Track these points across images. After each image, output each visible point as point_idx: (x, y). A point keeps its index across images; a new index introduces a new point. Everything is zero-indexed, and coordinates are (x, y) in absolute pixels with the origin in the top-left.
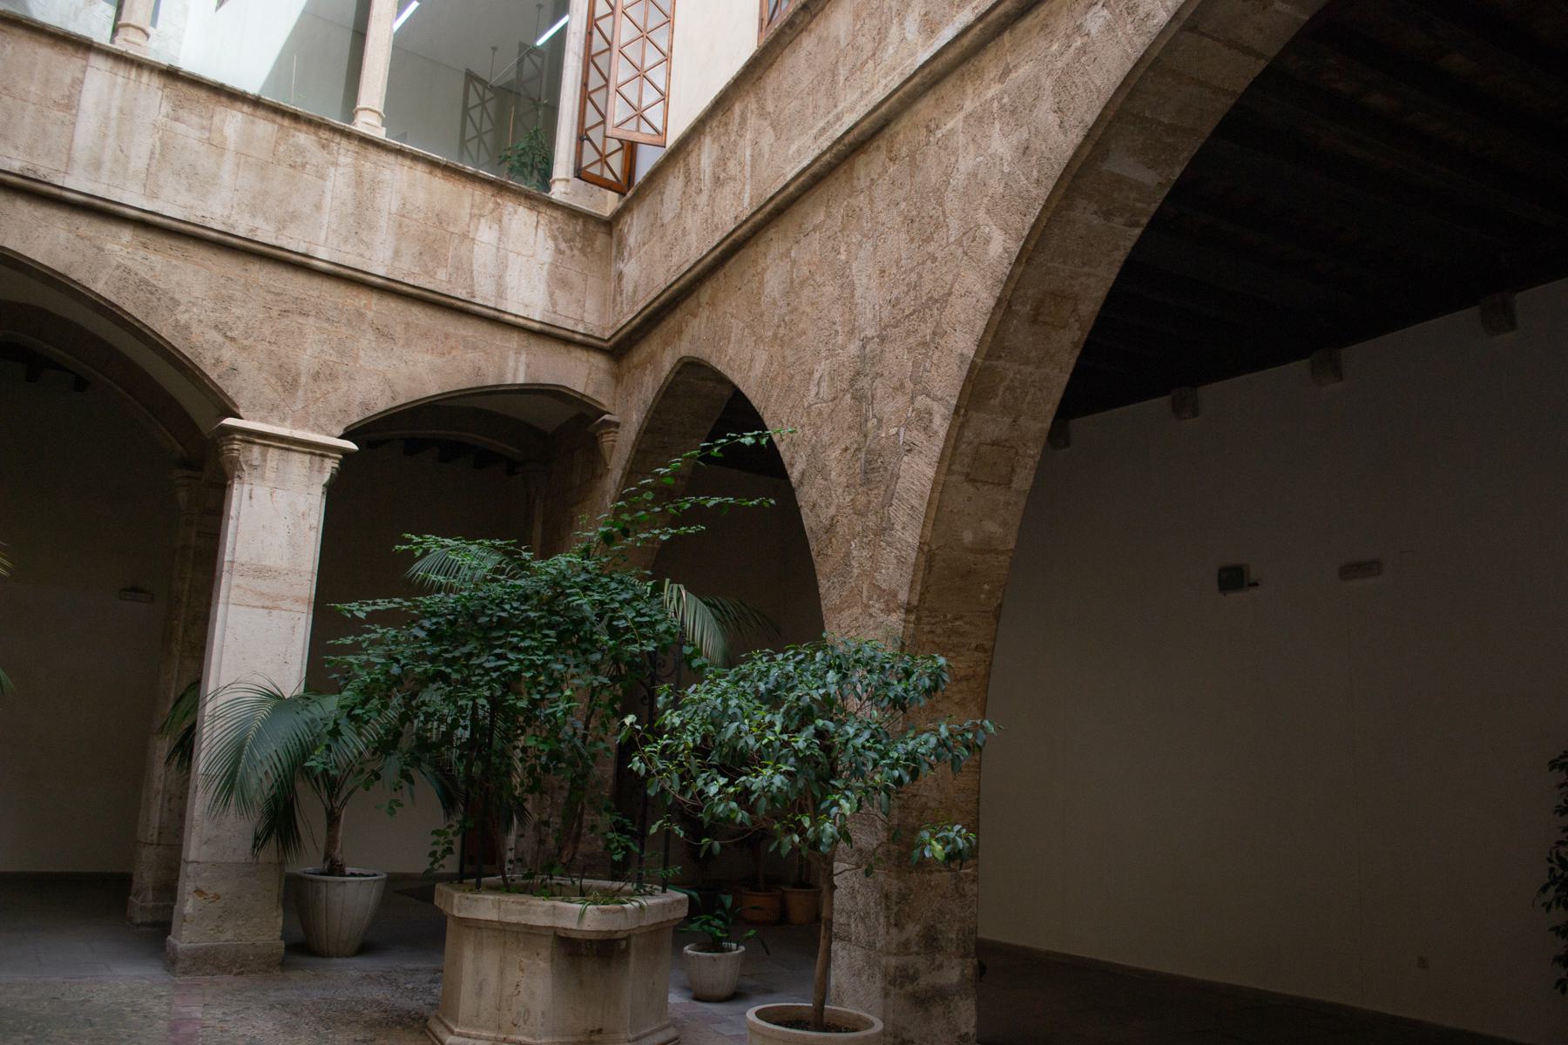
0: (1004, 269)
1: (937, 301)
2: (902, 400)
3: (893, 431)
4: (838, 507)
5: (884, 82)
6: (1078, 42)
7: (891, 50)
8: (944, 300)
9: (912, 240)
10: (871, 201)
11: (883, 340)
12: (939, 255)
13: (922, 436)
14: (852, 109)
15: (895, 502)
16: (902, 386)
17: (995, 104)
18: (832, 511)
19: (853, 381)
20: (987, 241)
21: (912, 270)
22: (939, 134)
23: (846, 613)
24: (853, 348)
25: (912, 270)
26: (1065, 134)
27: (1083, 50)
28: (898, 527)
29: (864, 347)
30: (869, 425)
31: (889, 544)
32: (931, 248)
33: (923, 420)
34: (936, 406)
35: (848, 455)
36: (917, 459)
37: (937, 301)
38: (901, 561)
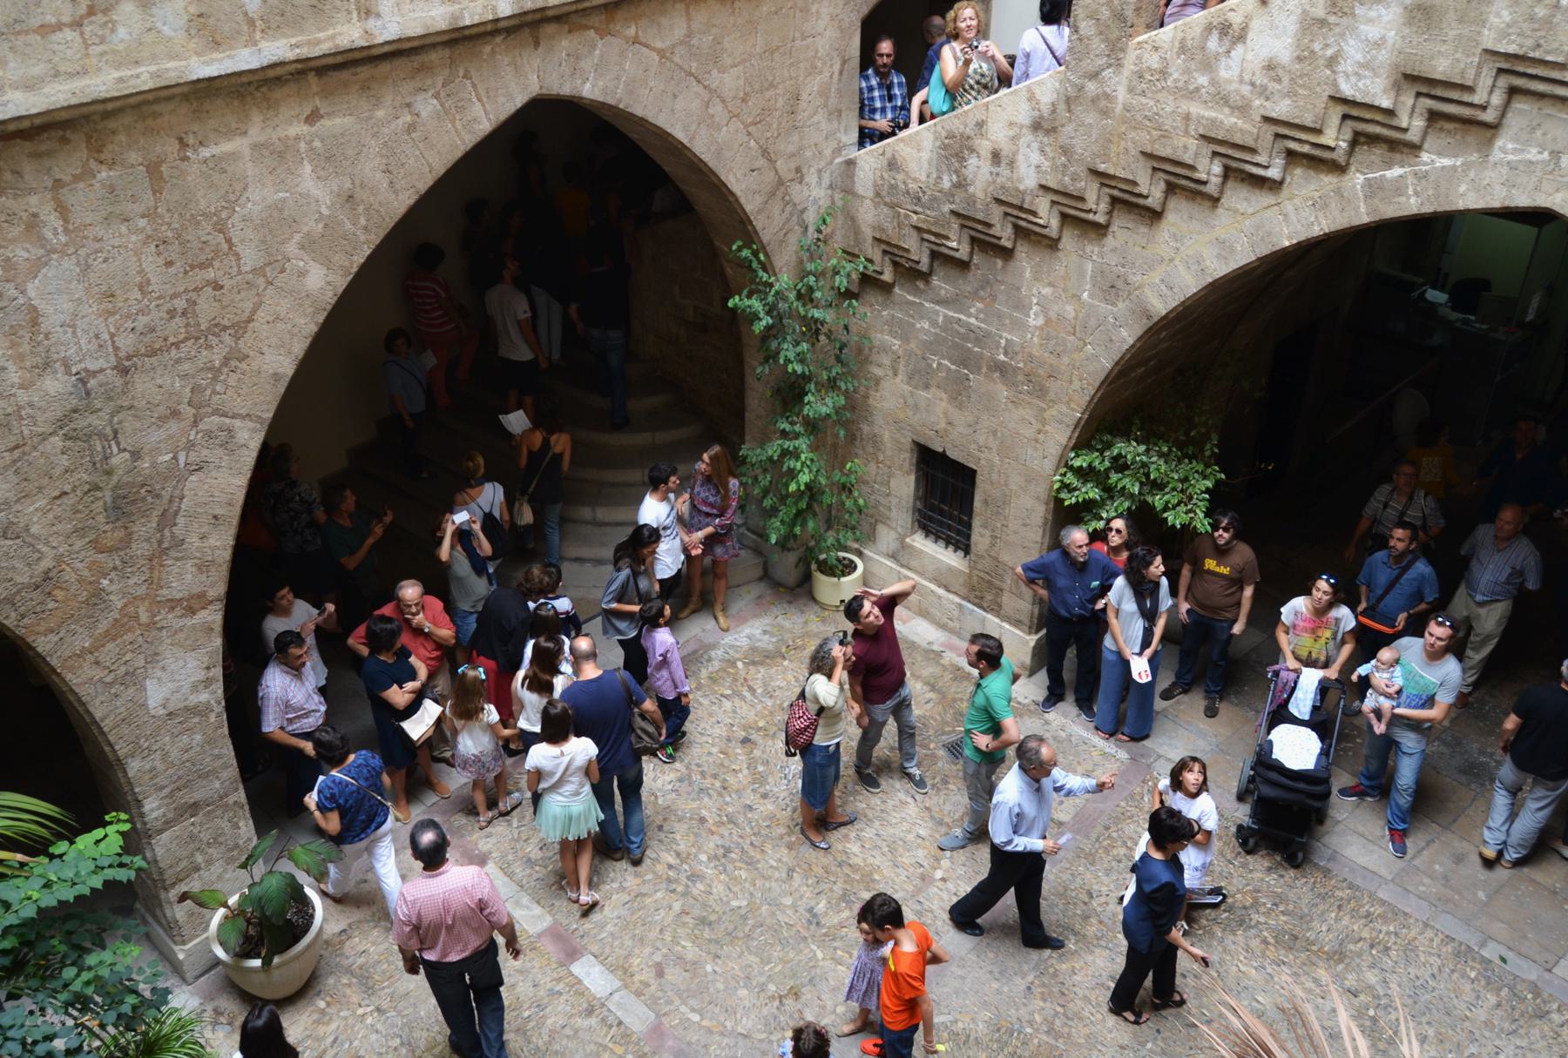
0: (330, 298)
1: (225, 328)
2: (174, 426)
3: (167, 457)
4: (59, 559)
5: (116, 74)
6: (409, 118)
7: (122, 32)
8: (240, 328)
9: (169, 264)
10: (63, 210)
11: (124, 371)
12: (227, 283)
13: (219, 452)
14: (29, 86)
15: (180, 520)
16: (175, 414)
17: (303, 145)
18: (47, 563)
19: (60, 423)
20: (302, 274)
21: (174, 296)
22: (205, 153)
23: (110, 646)
24: (56, 385)
25: (174, 296)
26: (396, 193)
27: (411, 128)
28: (193, 540)
29: (83, 381)
30: (114, 461)
31: (177, 559)
32: (210, 274)
33: (227, 441)
34: (237, 423)
35: (70, 501)
36: (214, 474)
37: (225, 328)
38: (202, 567)
